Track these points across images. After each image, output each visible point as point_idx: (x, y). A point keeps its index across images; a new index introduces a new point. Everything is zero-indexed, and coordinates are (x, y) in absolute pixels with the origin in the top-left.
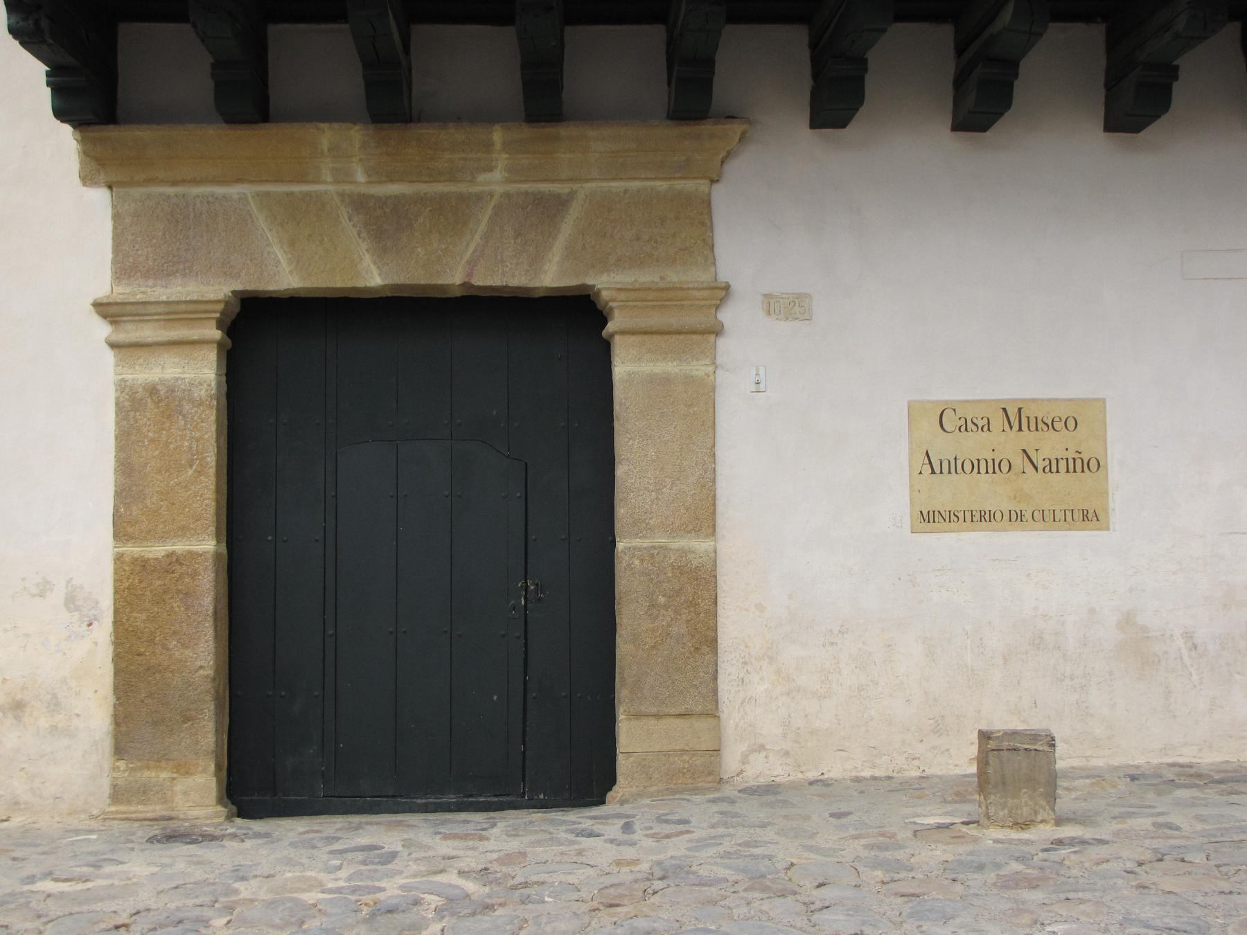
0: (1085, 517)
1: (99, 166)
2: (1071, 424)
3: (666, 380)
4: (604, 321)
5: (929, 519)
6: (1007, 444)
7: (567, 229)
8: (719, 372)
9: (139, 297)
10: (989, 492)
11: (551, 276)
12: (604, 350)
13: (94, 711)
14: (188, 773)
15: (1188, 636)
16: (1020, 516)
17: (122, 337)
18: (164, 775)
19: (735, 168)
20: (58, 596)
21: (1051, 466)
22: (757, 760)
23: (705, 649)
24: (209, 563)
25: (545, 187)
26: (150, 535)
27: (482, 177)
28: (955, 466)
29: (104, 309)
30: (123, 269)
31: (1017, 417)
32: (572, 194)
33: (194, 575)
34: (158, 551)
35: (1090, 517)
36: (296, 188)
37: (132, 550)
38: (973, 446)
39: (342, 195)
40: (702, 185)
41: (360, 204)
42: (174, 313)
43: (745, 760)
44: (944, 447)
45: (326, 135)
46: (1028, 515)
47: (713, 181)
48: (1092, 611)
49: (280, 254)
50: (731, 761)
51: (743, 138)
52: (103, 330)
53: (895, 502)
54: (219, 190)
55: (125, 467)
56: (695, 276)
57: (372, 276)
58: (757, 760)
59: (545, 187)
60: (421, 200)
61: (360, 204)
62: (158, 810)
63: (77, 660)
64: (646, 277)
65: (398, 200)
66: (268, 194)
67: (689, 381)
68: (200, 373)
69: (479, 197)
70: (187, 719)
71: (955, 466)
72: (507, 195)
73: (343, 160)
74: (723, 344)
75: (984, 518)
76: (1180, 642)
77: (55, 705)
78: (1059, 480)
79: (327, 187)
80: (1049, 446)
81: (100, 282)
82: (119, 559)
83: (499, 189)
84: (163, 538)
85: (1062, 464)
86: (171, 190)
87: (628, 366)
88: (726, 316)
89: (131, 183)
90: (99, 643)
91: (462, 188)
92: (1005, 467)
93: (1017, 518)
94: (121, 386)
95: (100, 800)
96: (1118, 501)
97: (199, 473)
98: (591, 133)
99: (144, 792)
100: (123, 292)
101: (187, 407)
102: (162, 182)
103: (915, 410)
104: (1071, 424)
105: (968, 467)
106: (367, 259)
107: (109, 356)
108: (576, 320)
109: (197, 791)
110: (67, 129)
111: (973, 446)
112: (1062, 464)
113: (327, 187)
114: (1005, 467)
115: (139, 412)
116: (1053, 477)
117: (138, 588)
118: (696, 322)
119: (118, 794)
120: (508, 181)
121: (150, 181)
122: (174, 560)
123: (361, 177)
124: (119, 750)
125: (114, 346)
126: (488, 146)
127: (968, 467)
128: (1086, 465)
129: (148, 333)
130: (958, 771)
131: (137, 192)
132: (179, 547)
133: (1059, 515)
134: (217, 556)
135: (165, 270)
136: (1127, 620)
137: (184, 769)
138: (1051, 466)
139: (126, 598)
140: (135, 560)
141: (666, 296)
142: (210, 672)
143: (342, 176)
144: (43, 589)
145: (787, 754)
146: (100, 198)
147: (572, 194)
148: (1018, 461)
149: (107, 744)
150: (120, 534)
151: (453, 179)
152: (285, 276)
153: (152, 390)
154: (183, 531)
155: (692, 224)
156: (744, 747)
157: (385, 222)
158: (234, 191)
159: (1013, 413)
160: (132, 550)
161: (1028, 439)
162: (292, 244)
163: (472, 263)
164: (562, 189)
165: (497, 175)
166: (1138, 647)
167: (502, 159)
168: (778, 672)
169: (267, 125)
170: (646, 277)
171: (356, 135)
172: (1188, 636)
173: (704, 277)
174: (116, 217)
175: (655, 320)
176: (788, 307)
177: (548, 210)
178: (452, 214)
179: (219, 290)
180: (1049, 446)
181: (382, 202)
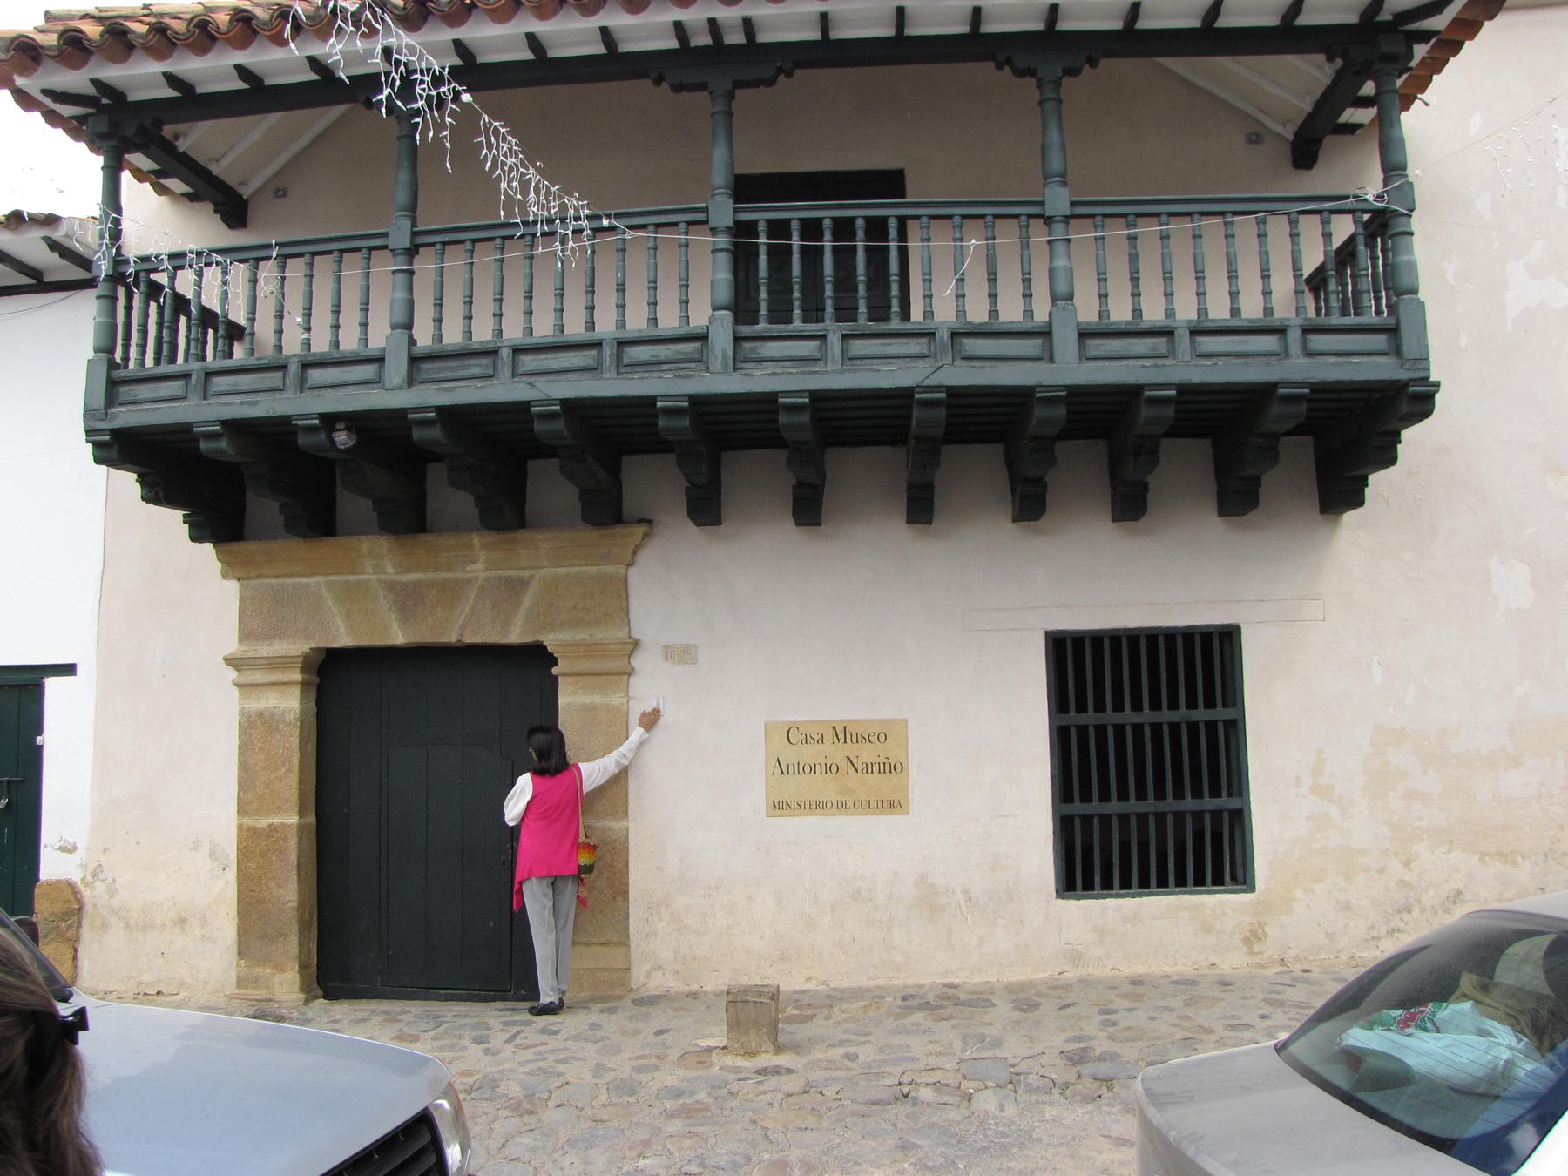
0: (892, 805)
1: (231, 567)
2: (882, 738)
3: (593, 708)
4: (555, 662)
5: (779, 807)
6: (835, 752)
7: (527, 601)
8: (632, 703)
9: (250, 654)
10: (823, 787)
11: (516, 635)
12: (551, 688)
13: (226, 927)
14: (282, 971)
15: (965, 891)
16: (845, 806)
17: (243, 680)
18: (268, 971)
19: (644, 556)
20: (205, 850)
21: (868, 769)
22: (657, 976)
23: (619, 898)
24: (294, 832)
25: (513, 573)
26: (259, 812)
27: (469, 568)
28: (798, 769)
29: (229, 661)
30: (246, 635)
31: (842, 733)
32: (531, 577)
33: (285, 839)
34: (263, 822)
35: (895, 805)
36: (350, 578)
37: (249, 821)
38: (811, 754)
39: (380, 581)
40: (621, 569)
41: (392, 587)
42: (273, 663)
43: (648, 976)
44: (790, 755)
45: (365, 544)
46: (850, 804)
47: (628, 566)
48: (896, 873)
49: (340, 623)
50: (638, 976)
51: (646, 535)
52: (232, 674)
53: (755, 796)
54: (304, 580)
55: (244, 767)
56: (615, 634)
57: (399, 638)
58: (657, 976)
59: (513, 573)
60: (431, 584)
61: (392, 587)
62: (264, 994)
63: (215, 890)
64: (579, 635)
65: (417, 585)
66: (334, 582)
67: (609, 708)
68: (289, 703)
69: (469, 581)
70: (281, 935)
71: (798, 769)
72: (487, 579)
73: (376, 561)
74: (635, 681)
75: (817, 806)
76: (960, 896)
77: (204, 922)
78: (873, 779)
79: (369, 576)
80: (866, 754)
81: (231, 644)
82: (240, 827)
83: (483, 575)
84: (266, 814)
85: (876, 768)
86: (274, 581)
87: (569, 698)
88: (637, 661)
89: (248, 578)
90: (226, 885)
91: (458, 575)
92: (834, 769)
93: (843, 806)
94: (242, 712)
95: (231, 987)
96: (915, 794)
97: (288, 770)
98: (540, 537)
99: (255, 982)
100: (250, 651)
101: (281, 726)
102: (267, 577)
103: (769, 728)
104: (882, 738)
105: (807, 769)
106: (395, 625)
107: (236, 690)
108: (537, 658)
109: (286, 984)
110: (208, 548)
111: (811, 754)
112: (876, 768)
113: (369, 576)
114: (834, 769)
115: (254, 728)
116: (868, 777)
117: (253, 846)
118: (617, 667)
119: (241, 982)
120: (487, 569)
121: (258, 577)
122: (273, 829)
123: (390, 570)
124: (241, 954)
125: (239, 686)
126: (471, 547)
127: (807, 769)
128: (894, 767)
129: (258, 677)
130: (797, 988)
131: (253, 583)
132: (276, 820)
133: (873, 804)
134: (301, 828)
135: (270, 634)
136: (922, 880)
137: (280, 968)
138: (868, 769)
139: (244, 853)
140: (249, 828)
141: (591, 649)
142: (295, 904)
143: (379, 569)
144: (197, 845)
145: (677, 972)
146: (233, 586)
147: (531, 577)
148: (844, 765)
149: (235, 948)
150: (242, 811)
151: (450, 570)
152: (343, 638)
153: (261, 715)
154: (278, 810)
155: (613, 600)
156: (648, 967)
157: (408, 600)
158: (313, 580)
159: (840, 730)
160: (249, 821)
161: (851, 749)
162: (348, 616)
163: (463, 627)
164: (525, 574)
165: (479, 566)
166: (930, 901)
167: (482, 556)
168: (672, 915)
169: (331, 540)
170: (579, 635)
171: (383, 543)
172: (965, 891)
173: (621, 634)
174: (241, 599)
175: (585, 665)
176: (681, 654)
177: (515, 587)
178: (451, 593)
179: (298, 648)
180: (866, 754)
181: (405, 585)
